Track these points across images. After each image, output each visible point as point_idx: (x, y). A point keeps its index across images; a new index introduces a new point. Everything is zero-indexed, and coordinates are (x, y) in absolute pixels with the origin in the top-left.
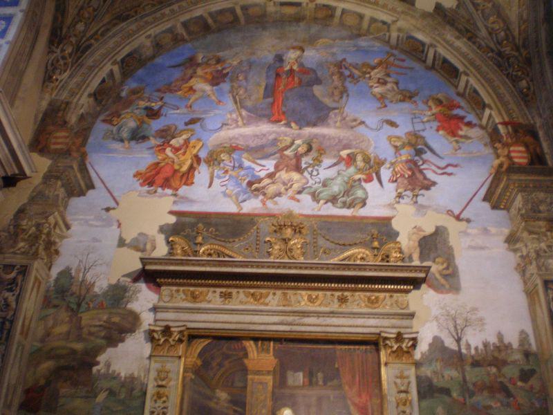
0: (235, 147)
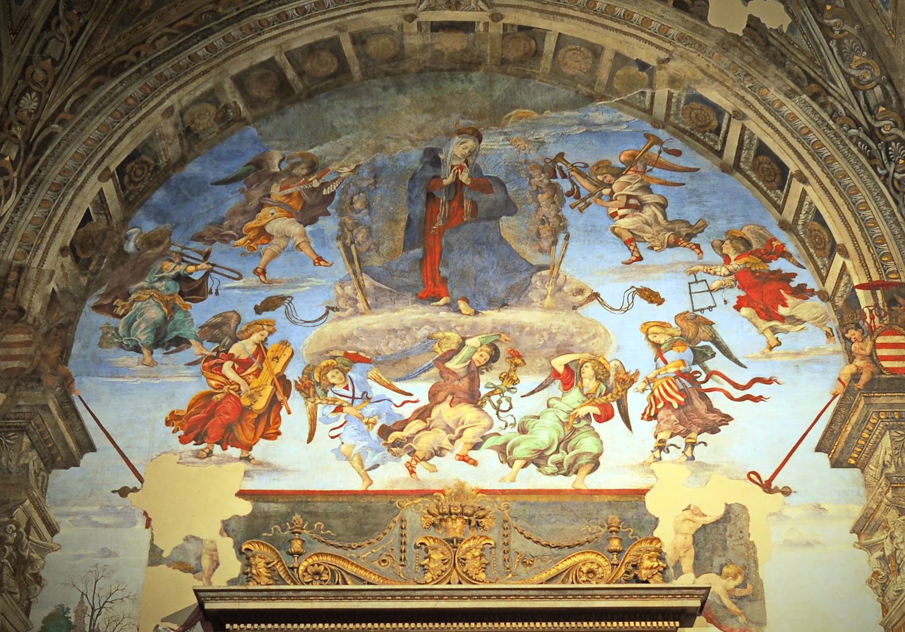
0: (357, 355)
